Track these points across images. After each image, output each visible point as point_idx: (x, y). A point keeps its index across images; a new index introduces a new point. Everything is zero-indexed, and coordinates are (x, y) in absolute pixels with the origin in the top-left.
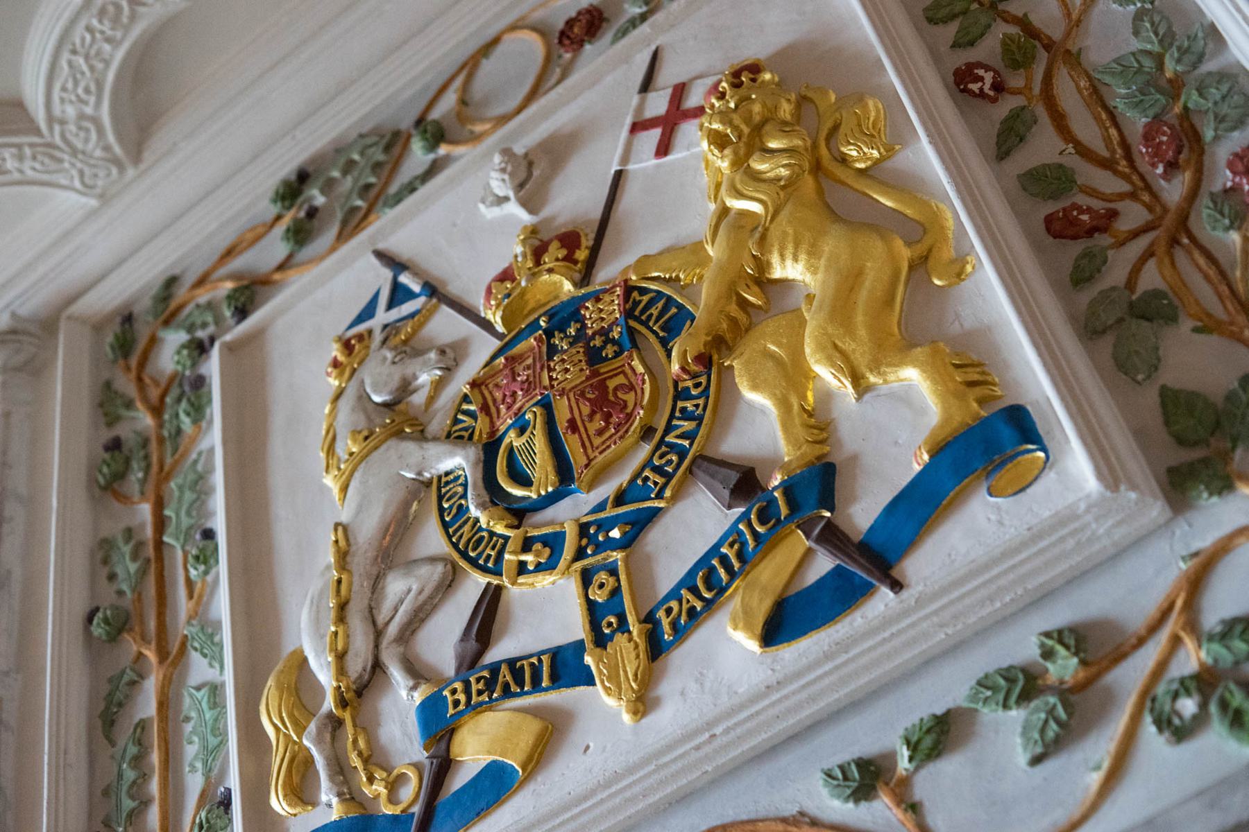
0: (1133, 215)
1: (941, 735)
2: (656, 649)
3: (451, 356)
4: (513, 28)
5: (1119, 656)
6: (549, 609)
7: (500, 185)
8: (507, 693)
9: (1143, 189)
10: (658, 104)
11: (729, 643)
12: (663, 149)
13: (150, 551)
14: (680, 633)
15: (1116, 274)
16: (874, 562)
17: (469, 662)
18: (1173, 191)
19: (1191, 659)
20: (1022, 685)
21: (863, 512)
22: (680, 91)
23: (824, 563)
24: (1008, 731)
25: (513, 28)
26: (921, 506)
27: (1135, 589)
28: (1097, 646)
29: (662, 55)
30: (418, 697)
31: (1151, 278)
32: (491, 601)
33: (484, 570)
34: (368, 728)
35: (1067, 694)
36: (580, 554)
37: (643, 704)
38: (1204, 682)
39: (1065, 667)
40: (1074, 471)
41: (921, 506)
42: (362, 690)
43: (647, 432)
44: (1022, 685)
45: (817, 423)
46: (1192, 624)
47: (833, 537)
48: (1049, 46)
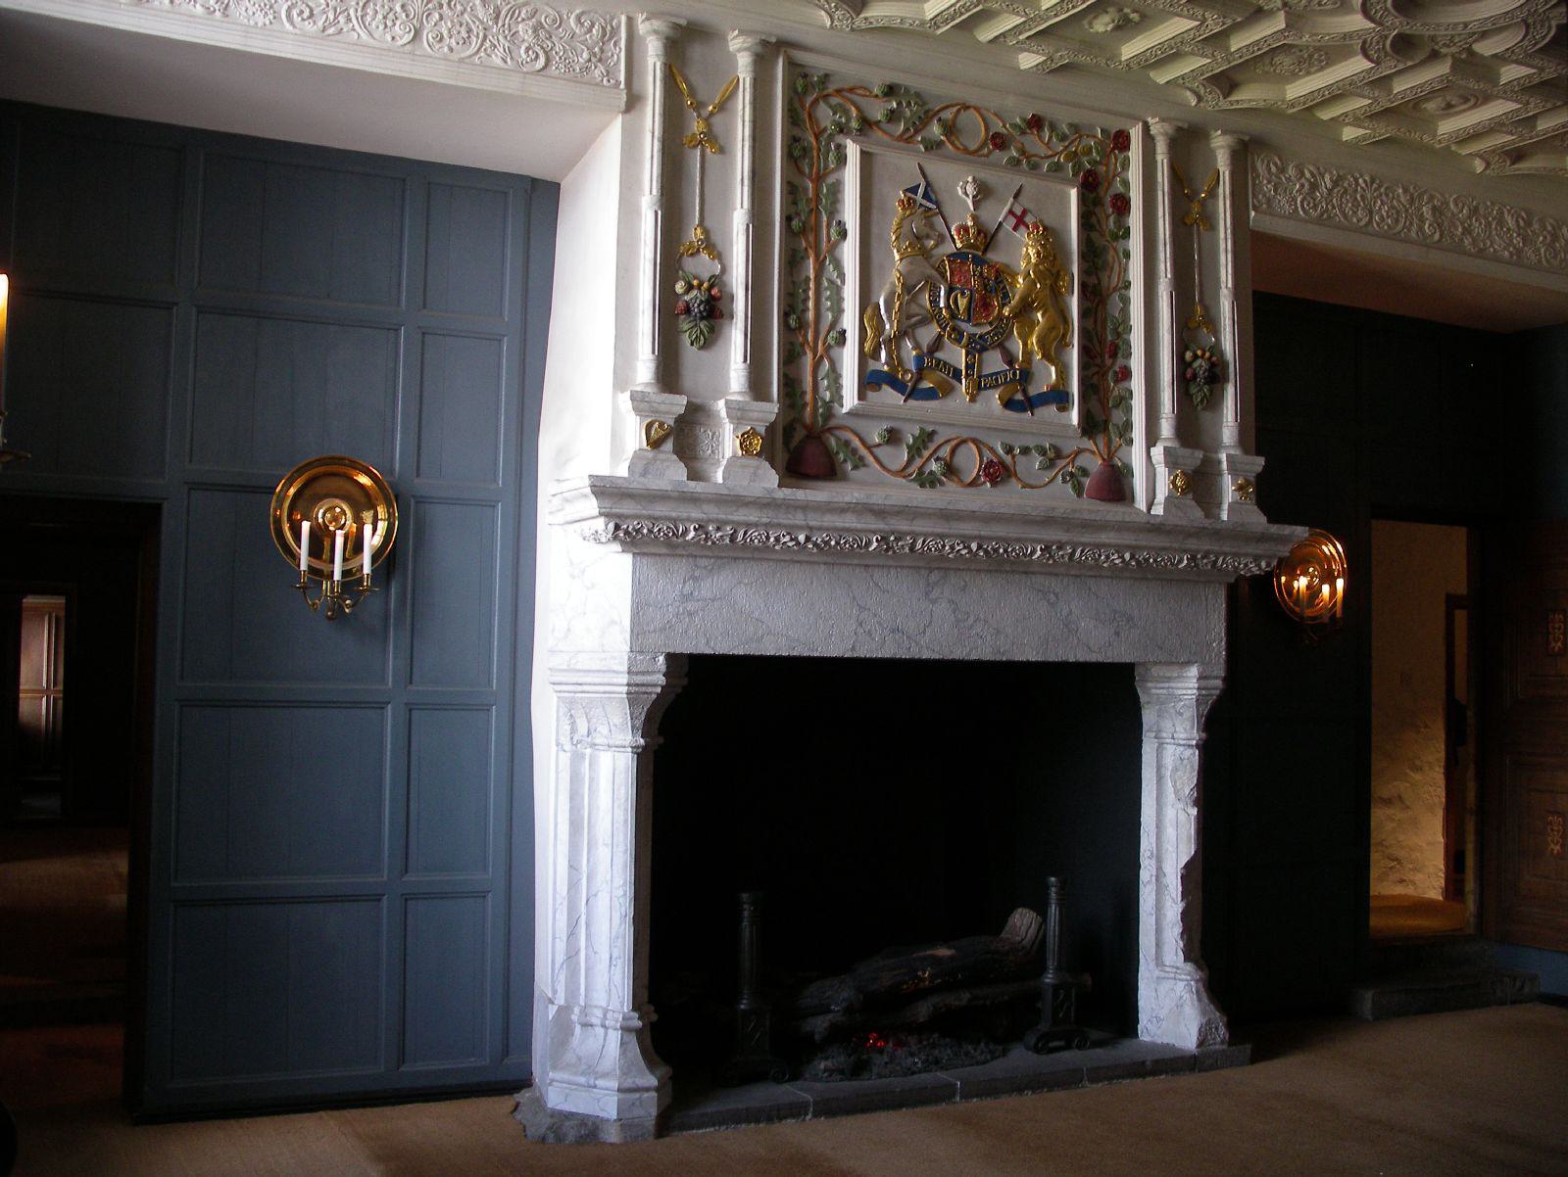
0: (1098, 361)
1: (1025, 451)
2: (979, 388)
3: (941, 239)
4: (977, 109)
6: (958, 356)
7: (970, 189)
8: (941, 371)
9: (1102, 356)
11: (994, 397)
12: (1015, 229)
13: (813, 205)
14: (986, 388)
16: (1030, 404)
18: (1108, 362)
21: (1033, 391)
23: (1019, 397)
24: (1037, 461)
25: (977, 109)
26: (1044, 399)
27: (1069, 447)
28: (1059, 454)
29: (1023, 190)
30: (914, 353)
31: (1095, 380)
32: (940, 337)
33: (940, 326)
34: (898, 348)
35: (1051, 460)
36: (967, 346)
37: (973, 400)
38: (1072, 475)
39: (1051, 454)
40: (1074, 416)
41: (1044, 399)
43: (991, 324)
44: (1043, 452)
45: (1028, 354)
46: (1073, 460)
47: (1024, 392)
48: (1101, 295)
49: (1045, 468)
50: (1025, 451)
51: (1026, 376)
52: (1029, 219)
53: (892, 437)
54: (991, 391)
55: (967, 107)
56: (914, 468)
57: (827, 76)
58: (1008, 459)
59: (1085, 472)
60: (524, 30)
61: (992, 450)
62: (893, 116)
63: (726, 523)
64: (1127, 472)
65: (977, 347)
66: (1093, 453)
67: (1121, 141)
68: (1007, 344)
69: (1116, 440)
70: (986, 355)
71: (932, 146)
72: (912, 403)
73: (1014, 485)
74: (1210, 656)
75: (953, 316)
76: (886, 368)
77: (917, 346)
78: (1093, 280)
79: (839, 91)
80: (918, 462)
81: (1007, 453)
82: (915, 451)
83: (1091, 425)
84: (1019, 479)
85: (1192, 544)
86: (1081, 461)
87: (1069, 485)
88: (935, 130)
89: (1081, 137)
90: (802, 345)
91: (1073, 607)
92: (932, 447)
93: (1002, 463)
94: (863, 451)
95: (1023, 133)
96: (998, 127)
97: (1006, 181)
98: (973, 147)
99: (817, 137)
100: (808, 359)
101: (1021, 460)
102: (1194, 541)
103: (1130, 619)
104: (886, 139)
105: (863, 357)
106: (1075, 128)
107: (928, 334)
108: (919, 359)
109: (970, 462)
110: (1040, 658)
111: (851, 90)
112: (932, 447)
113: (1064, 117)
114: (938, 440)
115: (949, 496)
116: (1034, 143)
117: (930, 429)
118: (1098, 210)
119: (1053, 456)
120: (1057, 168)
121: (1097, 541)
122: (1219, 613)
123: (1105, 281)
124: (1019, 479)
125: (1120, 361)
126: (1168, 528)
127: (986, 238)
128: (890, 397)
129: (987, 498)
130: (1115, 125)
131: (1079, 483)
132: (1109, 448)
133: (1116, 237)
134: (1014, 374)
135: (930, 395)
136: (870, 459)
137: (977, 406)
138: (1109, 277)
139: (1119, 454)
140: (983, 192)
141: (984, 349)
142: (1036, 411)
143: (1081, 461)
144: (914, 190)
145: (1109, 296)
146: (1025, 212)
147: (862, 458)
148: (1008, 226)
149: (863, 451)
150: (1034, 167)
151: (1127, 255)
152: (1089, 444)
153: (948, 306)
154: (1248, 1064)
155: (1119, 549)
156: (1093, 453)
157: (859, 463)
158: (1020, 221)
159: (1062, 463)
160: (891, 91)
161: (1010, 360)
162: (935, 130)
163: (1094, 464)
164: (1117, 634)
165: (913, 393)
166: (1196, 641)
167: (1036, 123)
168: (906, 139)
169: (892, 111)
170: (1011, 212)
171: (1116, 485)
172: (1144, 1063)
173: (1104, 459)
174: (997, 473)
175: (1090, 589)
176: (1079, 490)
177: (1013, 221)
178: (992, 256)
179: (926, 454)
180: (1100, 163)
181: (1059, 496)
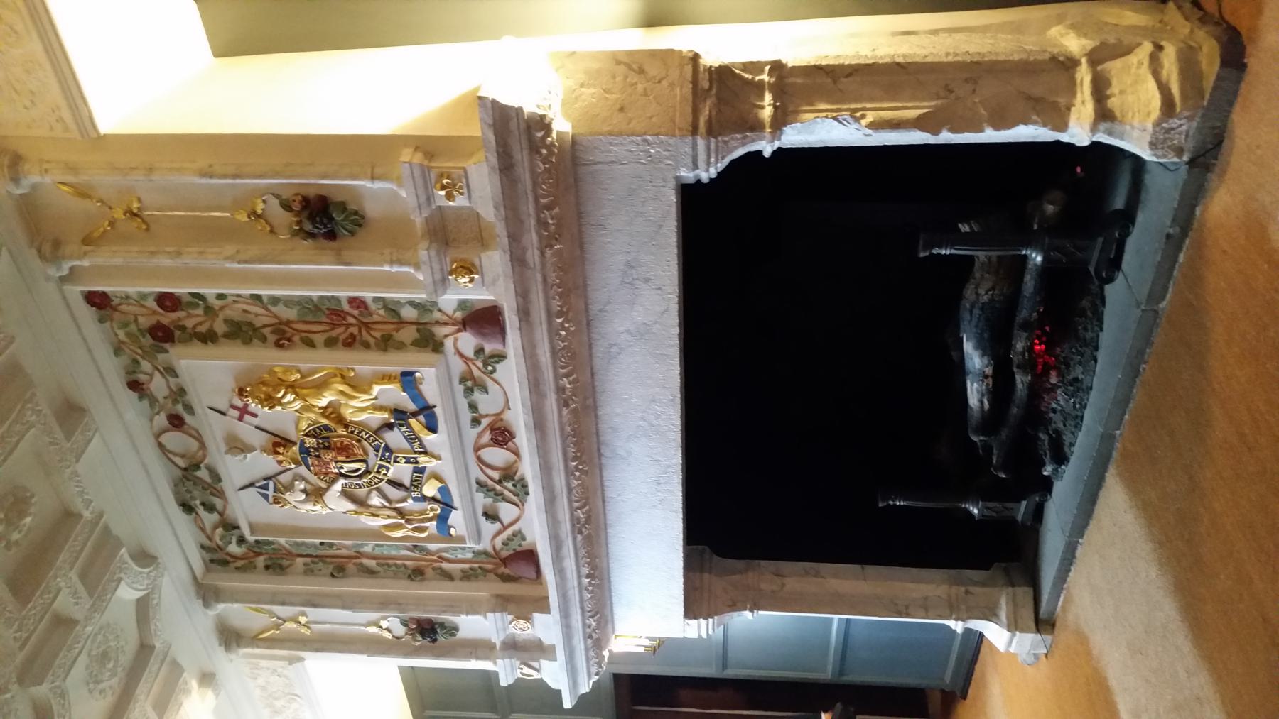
0: (354, 330)
1: (473, 407)
5: (471, 373)
10: (237, 413)
15: (372, 341)
17: (406, 489)
19: (480, 364)
20: (469, 391)
22: (233, 407)
24: (478, 396)
26: (416, 395)
27: (458, 366)
30: (410, 501)
31: (378, 335)
34: (411, 513)
38: (485, 364)
39: (469, 384)
42: (401, 513)
49: (485, 389)
50: (473, 407)
51: (400, 415)
52: (240, 404)
53: (491, 516)
54: (425, 443)
55: (161, 445)
56: (515, 499)
57: (202, 547)
58: (485, 422)
59: (479, 351)
60: (278, 704)
61: (480, 435)
62: (210, 508)
63: (584, 624)
64: (462, 304)
65: (388, 453)
66: (456, 340)
67: (98, 301)
68: (375, 425)
69: (437, 315)
70: (392, 446)
71: (216, 477)
72: (457, 503)
73: (507, 416)
74: (667, 158)
75: (367, 472)
76: (434, 523)
77: (404, 500)
78: (272, 338)
79: (210, 539)
80: (506, 493)
81: (479, 423)
82: (499, 496)
83: (429, 343)
84: (502, 412)
85: (533, 256)
86: (470, 353)
87: (497, 366)
88: (203, 474)
89: (123, 342)
90: (434, 569)
91: (622, 329)
92: (490, 482)
93: (492, 427)
94: (509, 532)
95: (153, 401)
96: (161, 420)
97: (214, 428)
98: (194, 445)
99: (260, 554)
100: (445, 565)
101: (483, 409)
102: (529, 255)
103: (629, 265)
104: (229, 507)
105: (430, 539)
106: (117, 351)
107: (393, 493)
108: (415, 499)
109: (497, 456)
110: (680, 636)
111: (203, 529)
112: (490, 482)
113: (113, 369)
114: (483, 478)
115: (528, 468)
116: (158, 385)
117: (475, 486)
118: (189, 323)
119: (471, 384)
120: (170, 371)
121: (550, 365)
122: (611, 144)
123: (266, 320)
124: (502, 412)
125: (346, 307)
126: (520, 300)
127: (279, 443)
128: (456, 518)
129: (524, 439)
130: (87, 314)
131: (492, 356)
132: (446, 324)
133: (209, 310)
134: (402, 425)
135: (444, 490)
136: (515, 528)
137: (443, 454)
138: (257, 315)
139: (450, 312)
140: (237, 446)
141: (387, 448)
142: (431, 402)
143: (470, 353)
144: (266, 497)
145: (276, 316)
146: (233, 407)
147: (514, 535)
148: (256, 421)
149: (509, 532)
150: (182, 391)
151: (221, 297)
152: (449, 343)
153: (360, 477)
154: (1239, 81)
155: (553, 332)
156: (456, 340)
157: (519, 535)
158: (244, 411)
159: (476, 373)
160: (187, 508)
161: (390, 426)
162: (203, 474)
163: (468, 341)
164: (647, 280)
165: (448, 506)
166: (649, 178)
167: (135, 385)
168: (221, 494)
169: (203, 504)
170: (241, 419)
171: (484, 319)
172: (1168, 236)
173: (459, 331)
174: (502, 435)
175: (600, 311)
176: (501, 357)
177: (247, 417)
178: (293, 438)
179: (498, 487)
180: (136, 320)
181: (511, 374)
